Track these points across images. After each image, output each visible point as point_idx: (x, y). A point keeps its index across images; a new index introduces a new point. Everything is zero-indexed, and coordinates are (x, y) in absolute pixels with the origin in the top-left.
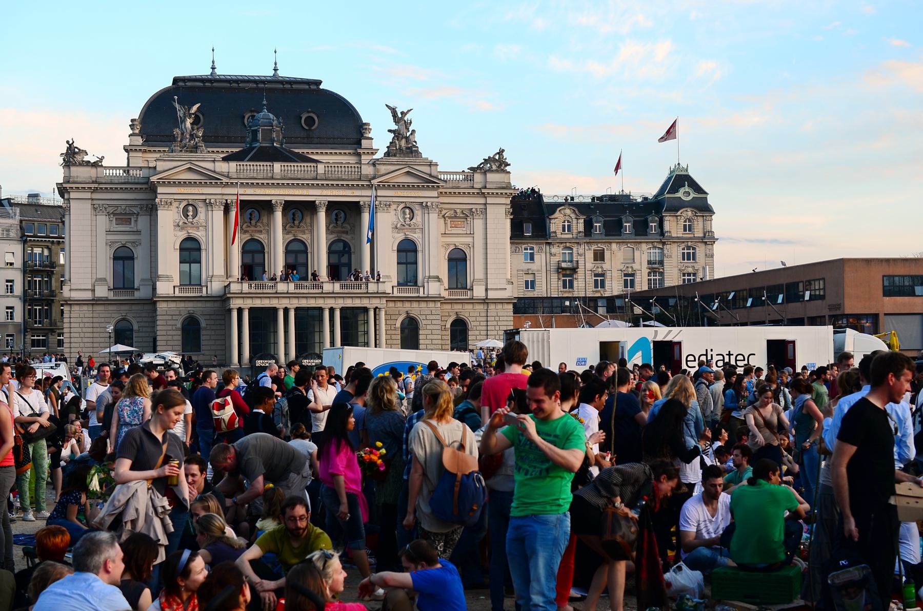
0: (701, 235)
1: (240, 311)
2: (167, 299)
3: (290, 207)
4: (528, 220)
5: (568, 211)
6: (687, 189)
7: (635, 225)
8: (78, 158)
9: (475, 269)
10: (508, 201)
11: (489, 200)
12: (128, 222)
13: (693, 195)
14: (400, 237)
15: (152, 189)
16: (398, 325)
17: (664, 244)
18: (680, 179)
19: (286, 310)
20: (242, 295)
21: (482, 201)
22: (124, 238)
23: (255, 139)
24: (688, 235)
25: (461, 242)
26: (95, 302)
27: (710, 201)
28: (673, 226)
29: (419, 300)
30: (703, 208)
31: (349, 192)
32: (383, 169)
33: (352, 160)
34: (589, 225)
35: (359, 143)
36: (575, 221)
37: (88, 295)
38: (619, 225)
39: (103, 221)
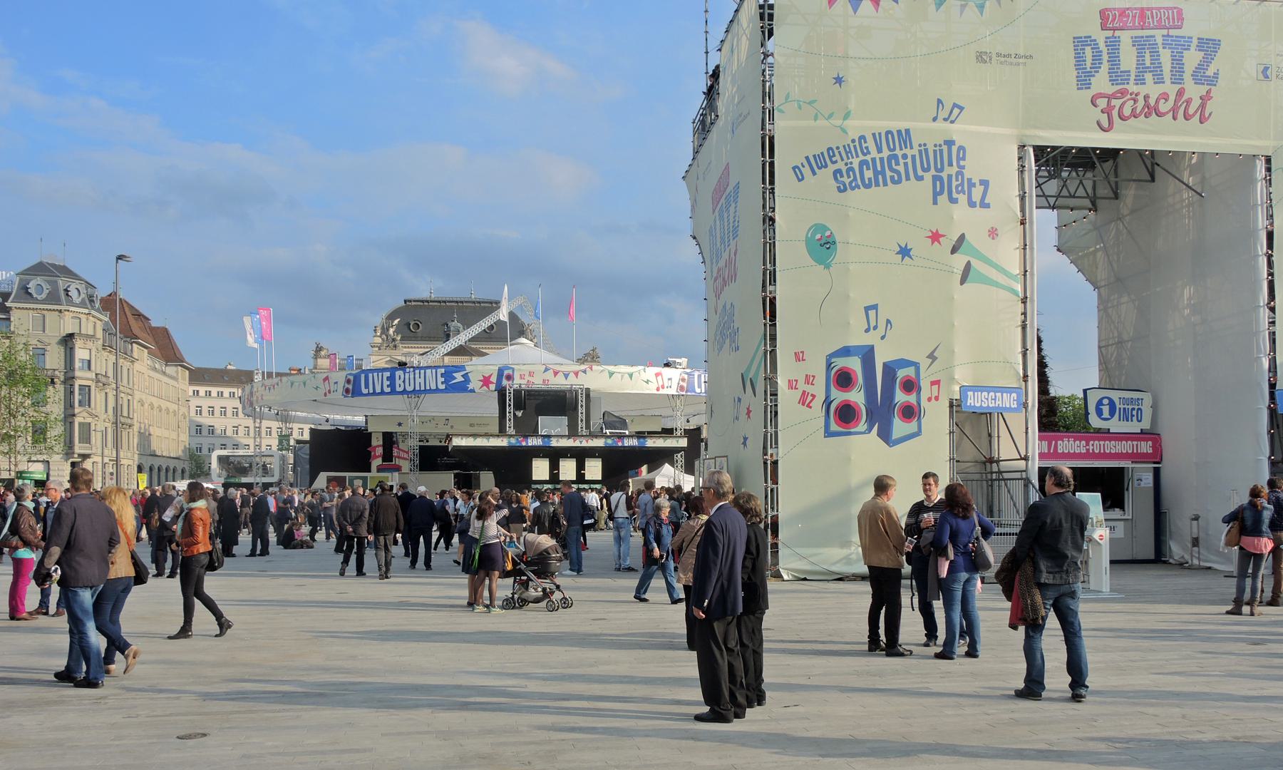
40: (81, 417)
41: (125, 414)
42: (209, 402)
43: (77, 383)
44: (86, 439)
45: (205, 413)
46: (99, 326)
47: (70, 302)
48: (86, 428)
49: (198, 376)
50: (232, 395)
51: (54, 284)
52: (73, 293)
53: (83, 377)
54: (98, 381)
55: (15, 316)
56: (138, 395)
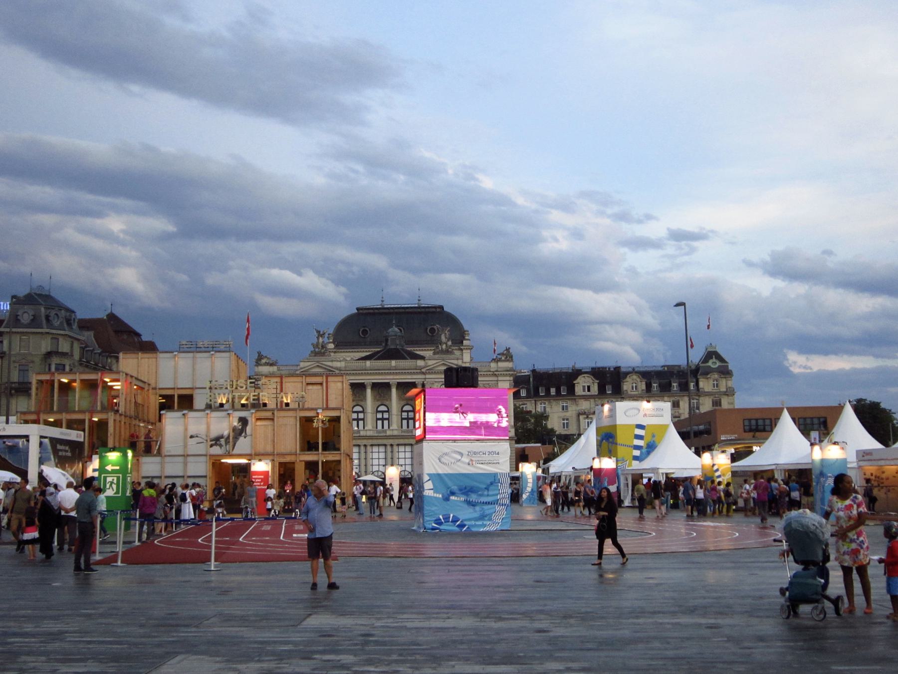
0: (725, 390)
3: (375, 386)
4: (610, 383)
5: (635, 377)
6: (714, 360)
7: (680, 385)
8: (264, 361)
10: (512, 378)
11: (500, 378)
13: (718, 364)
17: (699, 396)
18: (711, 355)
21: (495, 379)
23: (386, 345)
24: (716, 390)
27: (730, 368)
28: (705, 385)
30: (725, 372)
31: (409, 377)
32: (430, 363)
34: (649, 387)
36: (639, 384)
38: (670, 385)
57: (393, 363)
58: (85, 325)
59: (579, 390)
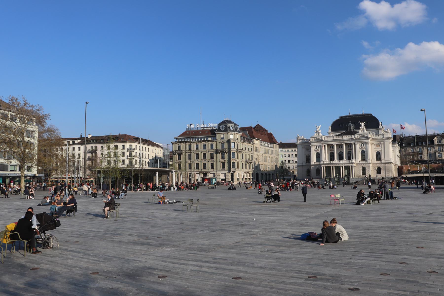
1: (324, 167)
2: (313, 165)
9: (382, 156)
12: (309, 150)
14: (361, 150)
15: (310, 143)
16: (361, 169)
19: (333, 167)
20: (324, 164)
22: (308, 153)
25: (379, 150)
26: (303, 166)
29: (365, 164)
33: (377, 131)
35: (378, 128)
37: (301, 165)
39: (304, 150)
40: (232, 161)
41: (251, 159)
42: (289, 153)
43: (231, 152)
44: (234, 167)
45: (287, 156)
46: (239, 136)
47: (230, 130)
48: (234, 164)
49: (283, 146)
50: (295, 151)
51: (226, 126)
52: (231, 128)
53: (233, 150)
54: (237, 151)
55: (217, 135)
56: (255, 153)
57: (344, 136)
58: (243, 129)
59: (436, 143)
